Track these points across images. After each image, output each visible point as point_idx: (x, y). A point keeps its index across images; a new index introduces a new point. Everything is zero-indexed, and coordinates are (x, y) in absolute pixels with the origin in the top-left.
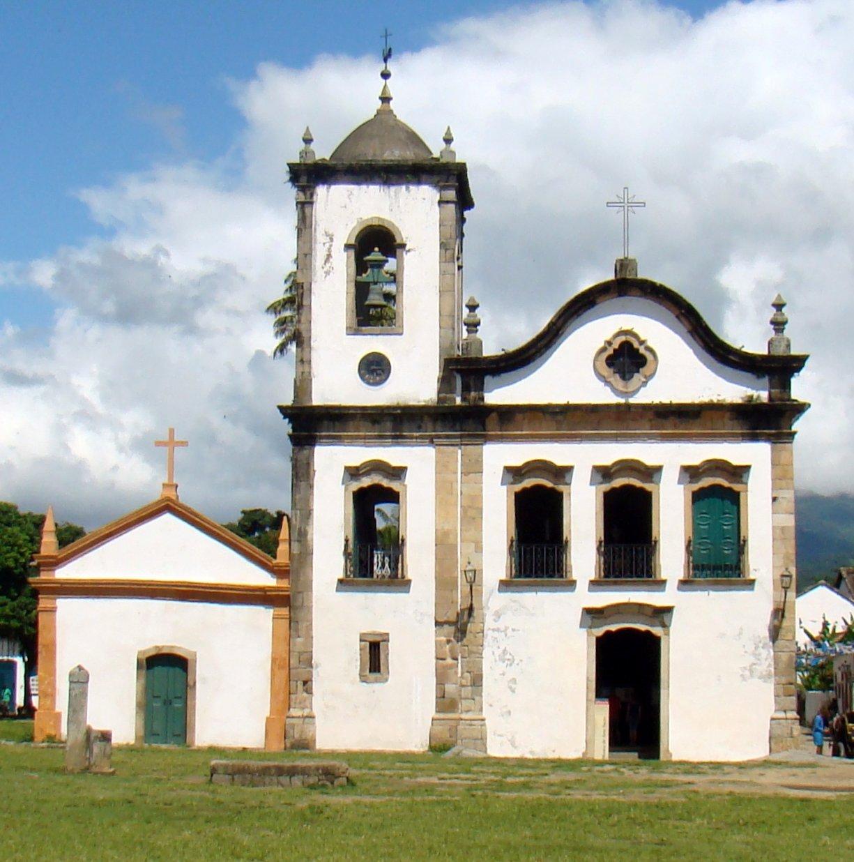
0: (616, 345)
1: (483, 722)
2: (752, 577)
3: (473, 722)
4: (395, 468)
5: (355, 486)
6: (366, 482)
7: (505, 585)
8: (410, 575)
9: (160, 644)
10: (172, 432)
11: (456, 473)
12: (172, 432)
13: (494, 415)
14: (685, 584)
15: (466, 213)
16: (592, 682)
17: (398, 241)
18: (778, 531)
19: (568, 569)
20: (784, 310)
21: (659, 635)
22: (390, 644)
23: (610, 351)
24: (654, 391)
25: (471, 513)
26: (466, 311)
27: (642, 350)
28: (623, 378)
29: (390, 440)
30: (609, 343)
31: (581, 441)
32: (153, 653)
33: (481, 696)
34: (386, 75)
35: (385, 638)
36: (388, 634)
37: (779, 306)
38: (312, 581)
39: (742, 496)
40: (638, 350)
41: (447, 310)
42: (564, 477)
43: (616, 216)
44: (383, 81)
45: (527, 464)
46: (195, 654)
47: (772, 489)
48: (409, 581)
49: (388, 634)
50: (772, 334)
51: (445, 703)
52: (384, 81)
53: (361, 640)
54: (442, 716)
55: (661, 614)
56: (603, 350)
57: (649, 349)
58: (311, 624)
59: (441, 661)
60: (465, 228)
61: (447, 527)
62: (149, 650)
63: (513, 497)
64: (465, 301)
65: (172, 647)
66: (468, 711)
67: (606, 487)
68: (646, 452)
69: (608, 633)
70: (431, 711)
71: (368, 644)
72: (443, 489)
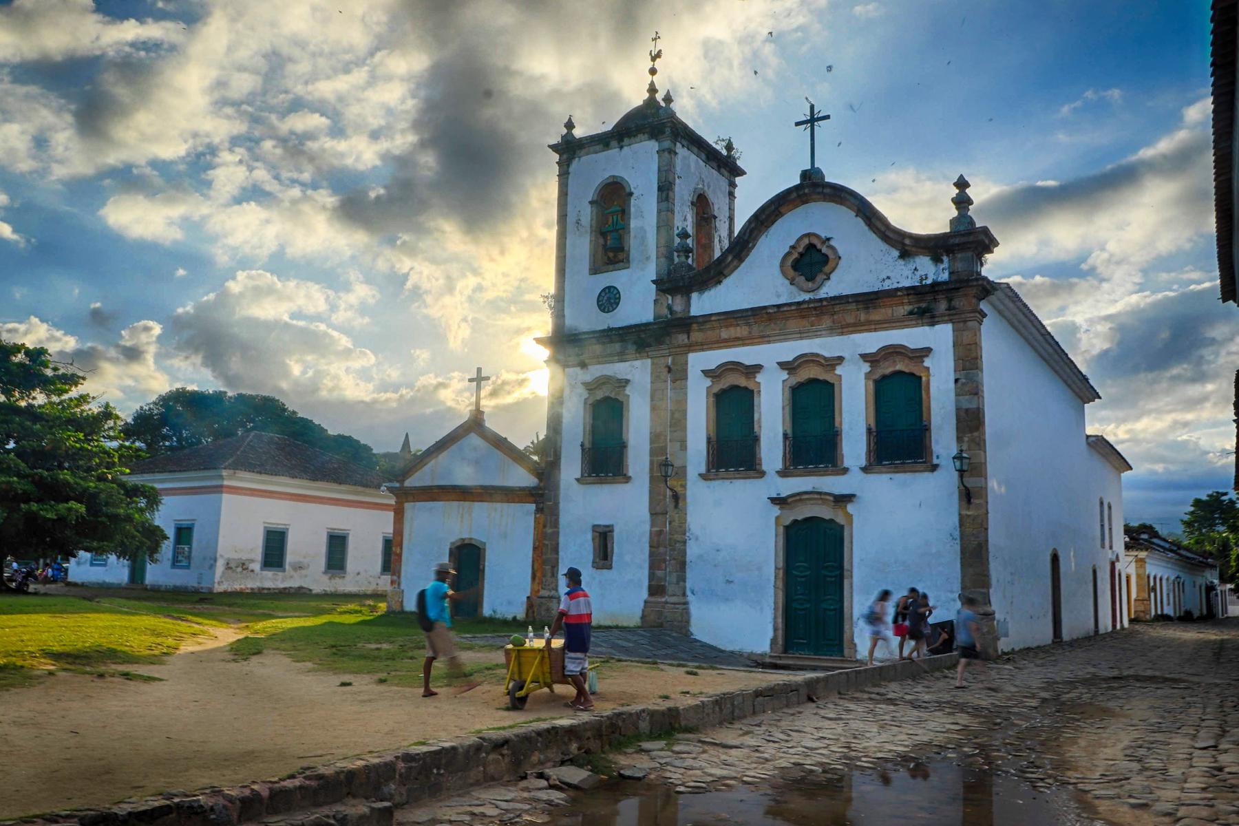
0: (801, 249)
1: (684, 607)
2: (935, 461)
3: (677, 606)
4: (619, 381)
5: (590, 401)
6: (600, 395)
7: (704, 477)
8: (630, 474)
9: (464, 537)
10: (479, 370)
11: (666, 381)
12: (479, 370)
13: (695, 326)
14: (865, 470)
15: (738, 180)
16: (779, 569)
17: (628, 190)
18: (962, 414)
19: (757, 462)
20: (967, 191)
21: (842, 523)
22: (615, 534)
23: (795, 255)
24: (838, 284)
25: (677, 415)
26: (677, 240)
27: (824, 250)
28: (808, 280)
29: (616, 358)
30: (793, 247)
31: (769, 342)
32: (459, 544)
33: (685, 582)
34: (653, 71)
35: (610, 528)
36: (613, 526)
37: (962, 184)
38: (559, 481)
39: (924, 379)
40: (820, 251)
41: (663, 241)
42: (755, 377)
43: (804, 132)
44: (649, 78)
45: (719, 367)
46: (485, 544)
47: (955, 371)
48: (630, 477)
49: (613, 526)
50: (955, 213)
51: (656, 589)
52: (651, 76)
53: (593, 531)
54: (653, 599)
55: (843, 500)
56: (788, 254)
57: (833, 248)
58: (558, 518)
59: (653, 550)
60: (737, 192)
61: (658, 431)
62: (457, 541)
63: (712, 399)
64: (676, 232)
65: (471, 539)
66: (674, 595)
67: (794, 380)
68: (824, 345)
69: (795, 521)
70: (645, 594)
71: (598, 534)
72: (655, 397)
